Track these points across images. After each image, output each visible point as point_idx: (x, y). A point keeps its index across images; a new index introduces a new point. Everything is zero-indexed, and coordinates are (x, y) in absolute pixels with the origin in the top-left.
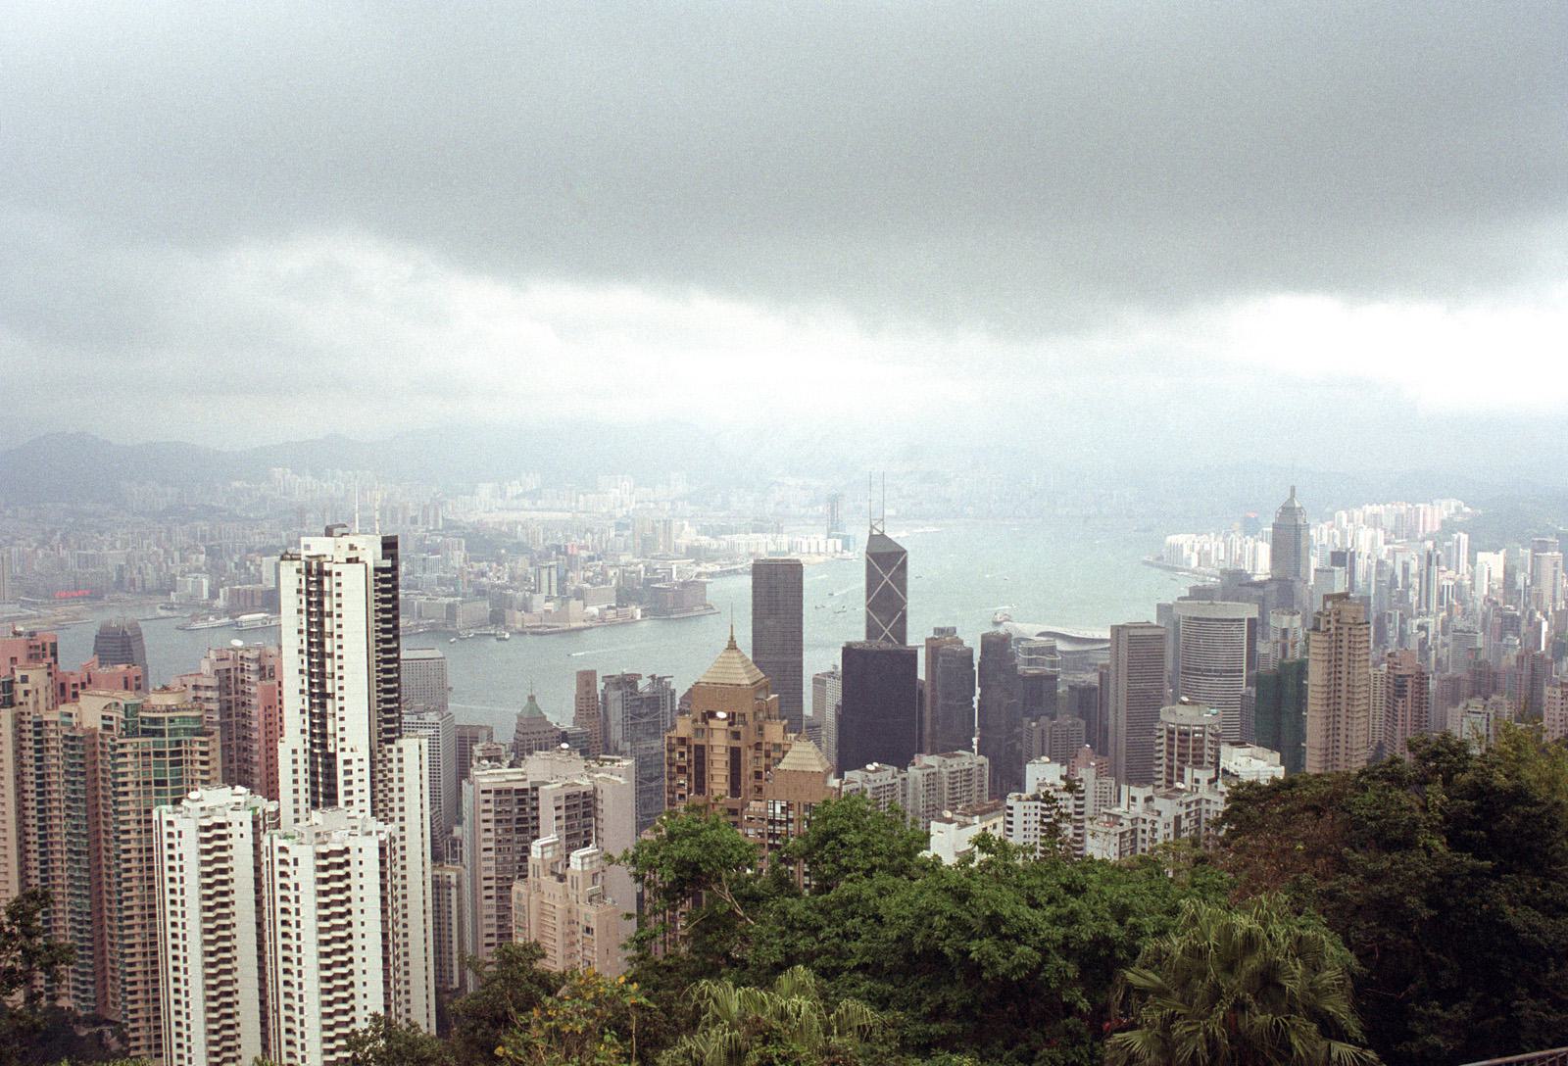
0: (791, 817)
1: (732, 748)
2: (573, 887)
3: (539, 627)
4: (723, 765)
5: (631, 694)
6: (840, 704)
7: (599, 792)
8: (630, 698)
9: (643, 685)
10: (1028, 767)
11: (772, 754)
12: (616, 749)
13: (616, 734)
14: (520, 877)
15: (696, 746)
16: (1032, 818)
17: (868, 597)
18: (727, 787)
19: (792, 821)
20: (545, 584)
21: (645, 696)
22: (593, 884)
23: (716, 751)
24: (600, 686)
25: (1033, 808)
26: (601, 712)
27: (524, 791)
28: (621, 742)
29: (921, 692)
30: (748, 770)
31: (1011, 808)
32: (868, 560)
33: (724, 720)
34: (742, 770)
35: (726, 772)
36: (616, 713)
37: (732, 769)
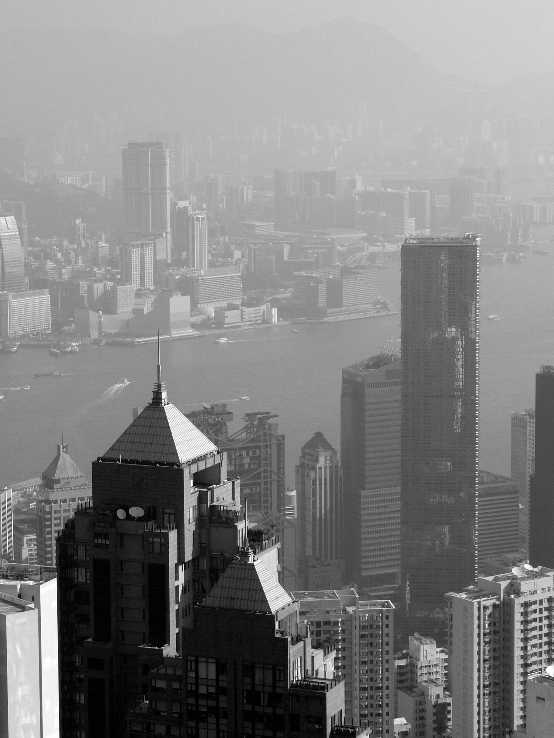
0: (222, 684)
20: (136, 272)
33: (140, 519)
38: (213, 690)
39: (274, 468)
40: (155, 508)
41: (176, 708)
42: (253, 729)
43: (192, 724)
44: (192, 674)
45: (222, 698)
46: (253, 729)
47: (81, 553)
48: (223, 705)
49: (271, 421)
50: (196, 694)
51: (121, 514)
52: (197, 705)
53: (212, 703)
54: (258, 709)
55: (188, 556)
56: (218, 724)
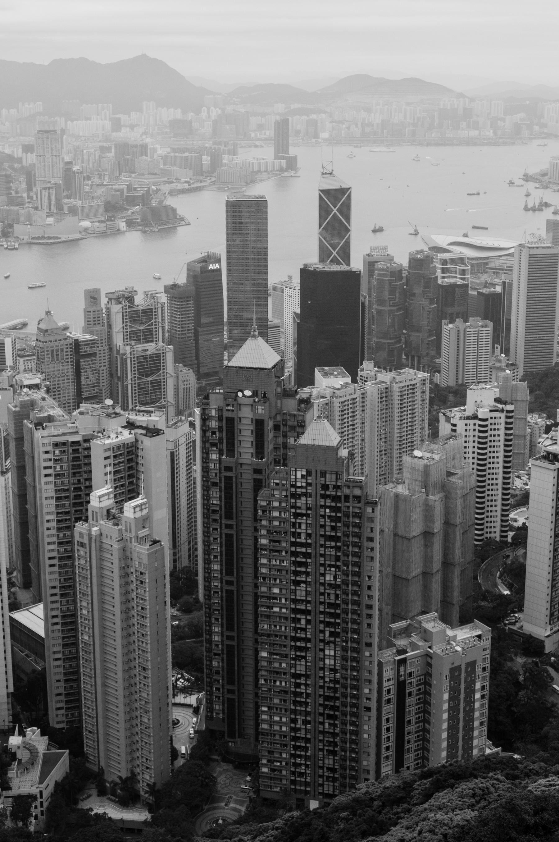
0: (309, 481)
1: (257, 420)
2: (126, 531)
3: (43, 238)
4: (249, 433)
5: (130, 307)
6: (298, 311)
7: (140, 443)
8: (128, 310)
9: (139, 300)
10: (469, 392)
11: (289, 423)
12: (118, 352)
13: (118, 340)
14: (78, 519)
15: (227, 418)
16: (471, 433)
17: (320, 227)
18: (252, 450)
19: (309, 484)
21: (140, 308)
22: (144, 527)
23: (244, 421)
24: (104, 300)
25: (472, 425)
26: (105, 321)
27: (78, 442)
28: (121, 347)
29: (363, 304)
30: (270, 435)
31: (455, 425)
32: (320, 196)
33: (249, 397)
34: (265, 439)
35: (252, 439)
36: (118, 324)
37: (257, 436)
38: (304, 484)
39: (160, 320)
40: (257, 391)
41: (284, 493)
42: (325, 502)
43: (293, 501)
44: (294, 477)
45: (309, 488)
46: (325, 502)
47: (213, 413)
48: (309, 491)
49: (158, 295)
50: (294, 486)
51: (240, 394)
52: (296, 491)
53: (304, 491)
54: (328, 493)
55: (273, 414)
56: (307, 500)
